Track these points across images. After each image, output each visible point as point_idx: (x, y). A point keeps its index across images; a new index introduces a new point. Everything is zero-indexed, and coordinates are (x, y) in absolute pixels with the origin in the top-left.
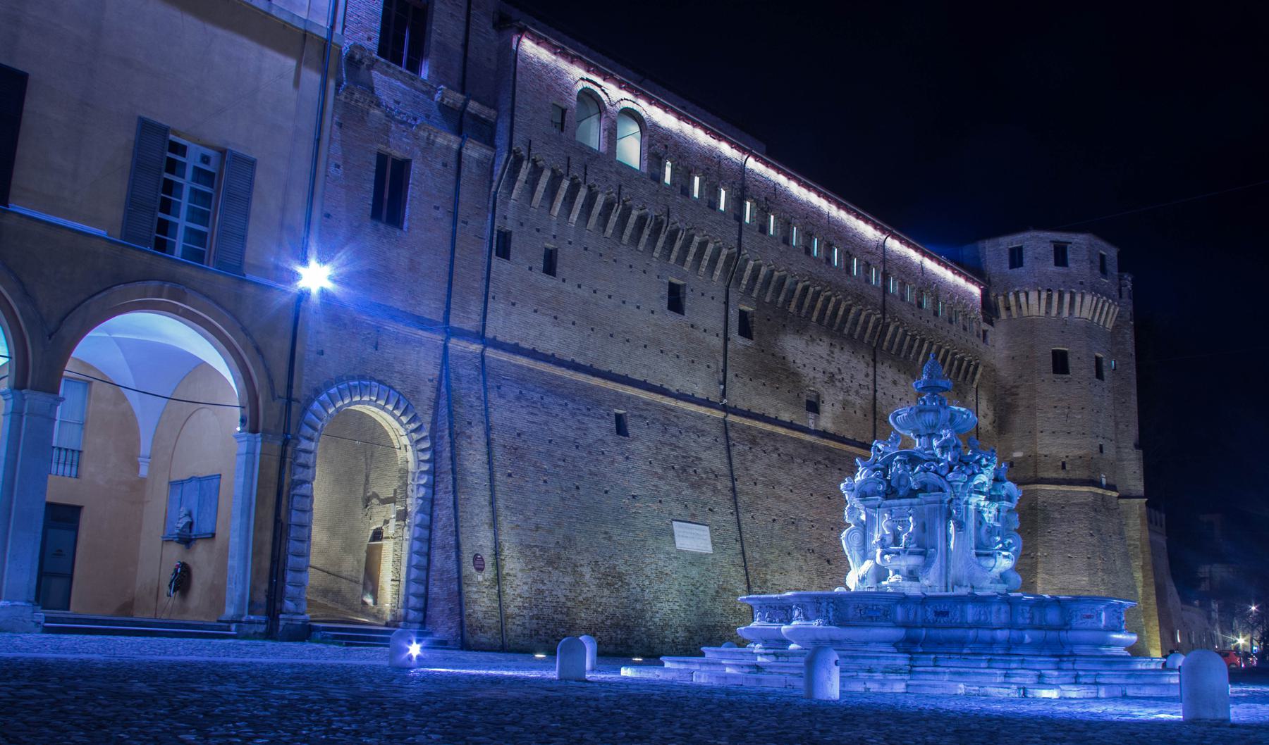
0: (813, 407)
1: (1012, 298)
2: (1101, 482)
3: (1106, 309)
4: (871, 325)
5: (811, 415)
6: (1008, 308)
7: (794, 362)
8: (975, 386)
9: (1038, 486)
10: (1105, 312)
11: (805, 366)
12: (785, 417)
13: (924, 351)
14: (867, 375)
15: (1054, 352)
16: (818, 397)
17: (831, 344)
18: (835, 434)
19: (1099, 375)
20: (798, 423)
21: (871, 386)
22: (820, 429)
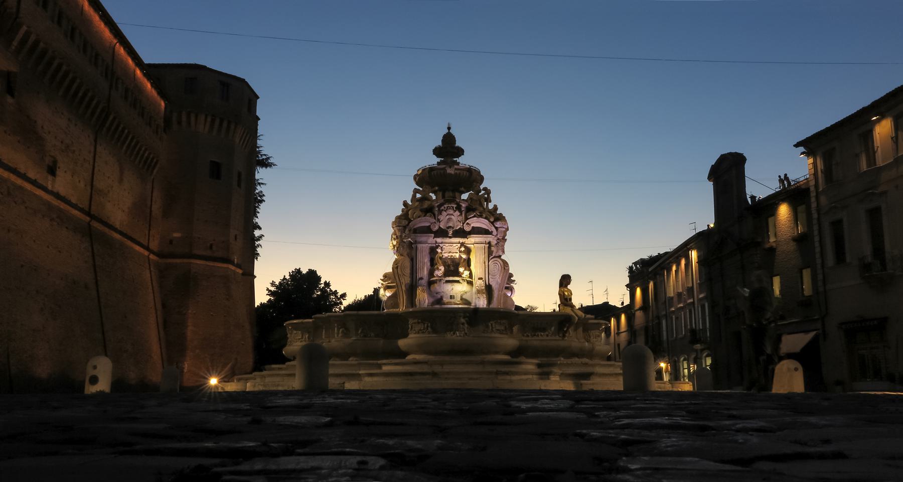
0: (52, 171)
1: (184, 118)
2: (234, 263)
3: (247, 138)
4: (99, 110)
5: (50, 177)
6: (179, 123)
7: (42, 127)
8: (152, 177)
9: (192, 261)
10: (246, 140)
11: (49, 132)
12: (31, 175)
13: (127, 142)
14: (90, 152)
15: (211, 162)
16: (55, 162)
17: (69, 119)
18: (64, 197)
19: (239, 185)
20: (40, 182)
21: (91, 163)
22: (55, 190)
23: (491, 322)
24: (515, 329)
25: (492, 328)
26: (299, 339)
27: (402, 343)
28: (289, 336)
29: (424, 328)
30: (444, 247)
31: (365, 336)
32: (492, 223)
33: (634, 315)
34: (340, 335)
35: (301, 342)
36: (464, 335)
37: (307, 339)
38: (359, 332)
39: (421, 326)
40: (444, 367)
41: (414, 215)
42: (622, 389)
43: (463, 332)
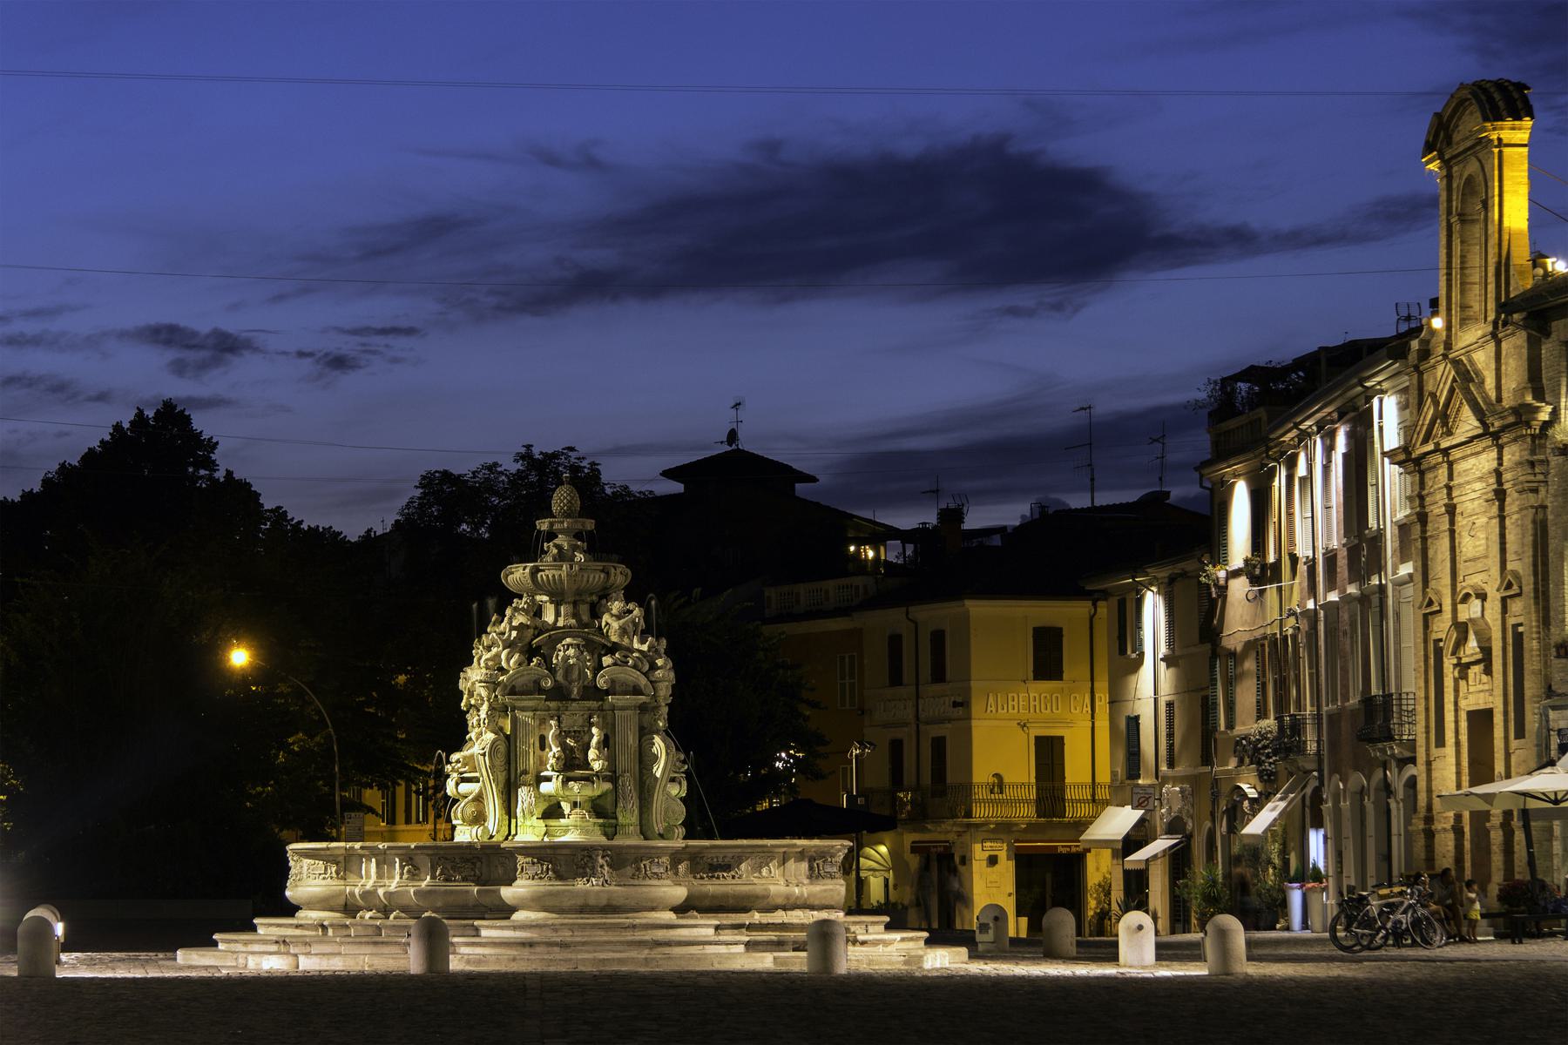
23: (644, 862)
24: (682, 868)
25: (645, 871)
26: (320, 874)
27: (507, 893)
28: (291, 863)
29: (542, 870)
30: (563, 716)
31: (447, 880)
32: (645, 674)
33: (1223, 590)
34: (405, 876)
35: (324, 878)
36: (603, 885)
37: (334, 875)
38: (437, 874)
39: (537, 868)
40: (576, 934)
41: (512, 662)
42: (1026, 918)
43: (602, 879)
